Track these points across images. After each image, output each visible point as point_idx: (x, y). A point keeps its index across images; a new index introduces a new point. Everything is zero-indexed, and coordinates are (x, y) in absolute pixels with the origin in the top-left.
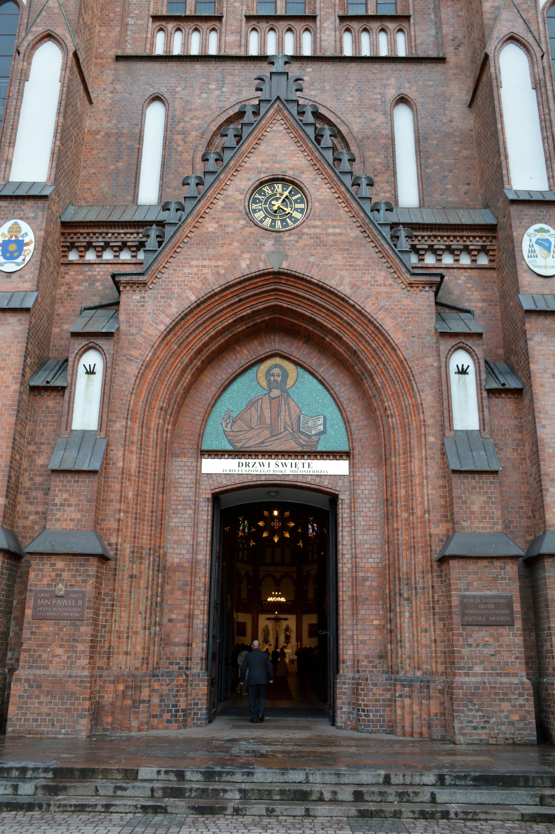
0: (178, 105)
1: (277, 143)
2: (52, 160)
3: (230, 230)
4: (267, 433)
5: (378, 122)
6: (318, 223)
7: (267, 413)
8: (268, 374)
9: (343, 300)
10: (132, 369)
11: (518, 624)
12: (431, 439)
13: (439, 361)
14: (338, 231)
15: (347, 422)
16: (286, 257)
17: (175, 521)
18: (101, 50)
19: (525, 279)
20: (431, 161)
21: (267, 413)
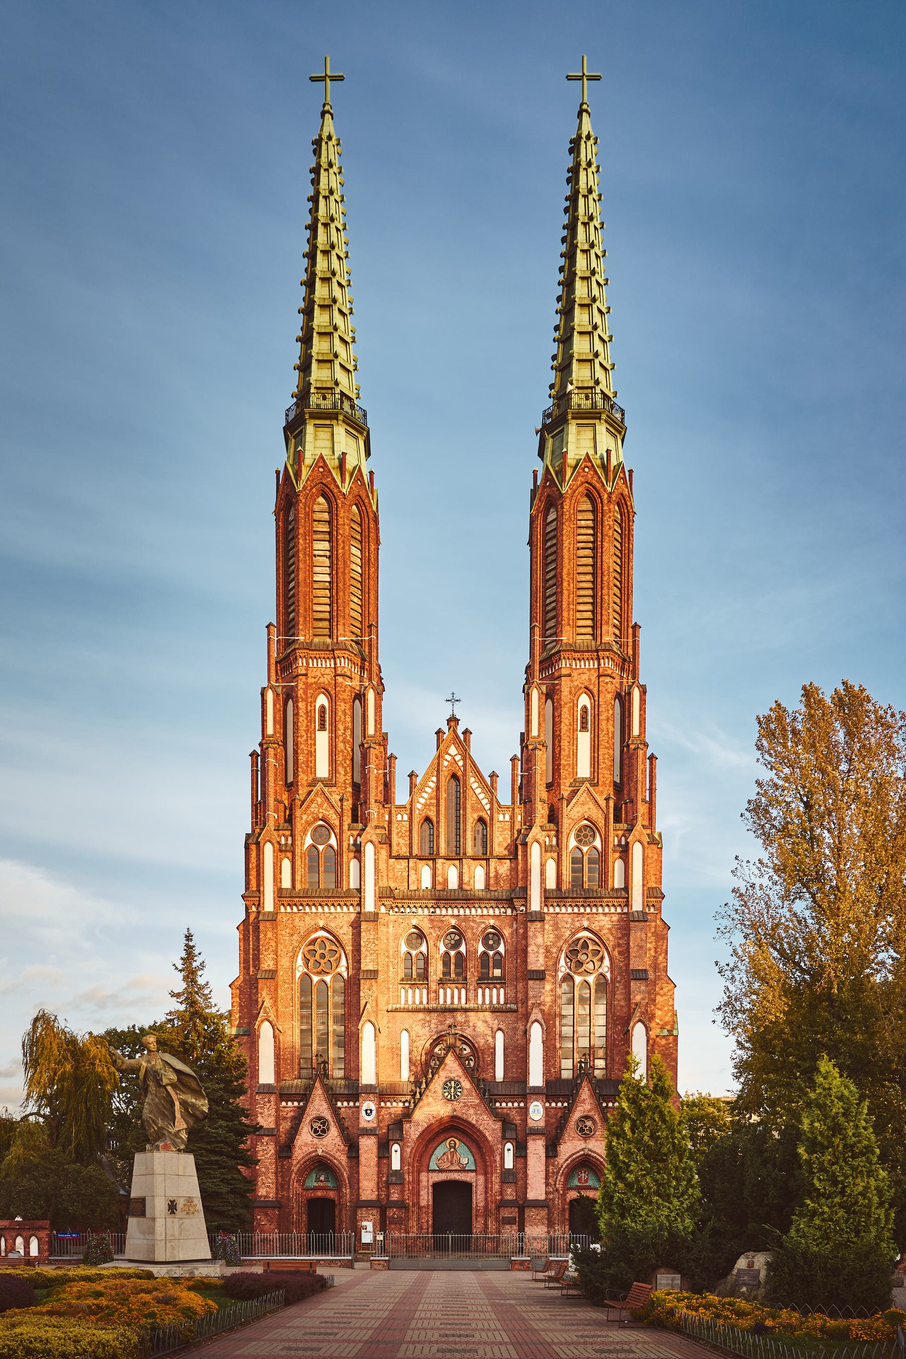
0: (413, 1034)
7: (450, 1157)
8: (450, 1143)
9: (473, 1126)
10: (409, 1150)
15: (475, 1160)
17: (422, 1193)
19: (529, 1121)
21: (450, 1157)
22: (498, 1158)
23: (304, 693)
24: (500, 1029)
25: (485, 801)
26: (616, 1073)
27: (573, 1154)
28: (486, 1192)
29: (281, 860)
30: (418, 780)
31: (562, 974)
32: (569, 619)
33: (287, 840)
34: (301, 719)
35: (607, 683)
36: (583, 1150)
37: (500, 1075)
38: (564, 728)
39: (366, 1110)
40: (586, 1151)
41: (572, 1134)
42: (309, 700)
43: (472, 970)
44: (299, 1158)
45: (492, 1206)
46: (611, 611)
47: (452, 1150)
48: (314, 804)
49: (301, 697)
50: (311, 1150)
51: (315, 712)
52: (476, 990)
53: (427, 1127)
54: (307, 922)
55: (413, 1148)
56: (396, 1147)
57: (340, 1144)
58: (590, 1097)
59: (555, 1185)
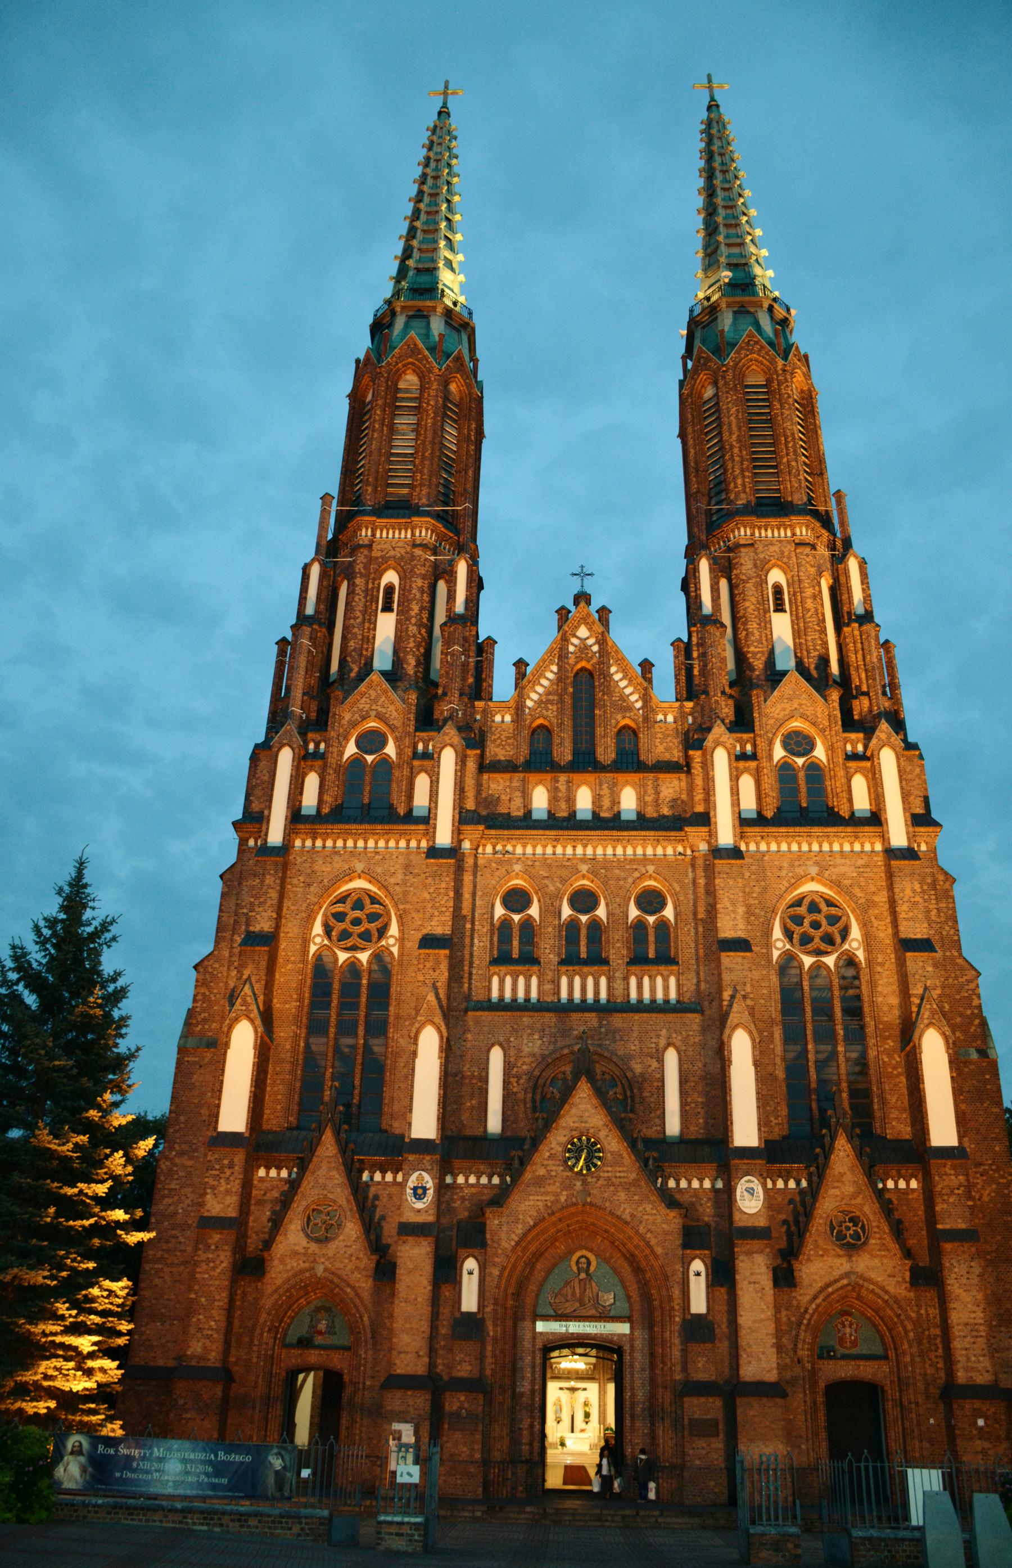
0: (512, 1052)
1: (582, 1107)
2: (438, 1124)
3: (553, 1173)
4: (577, 1304)
5: (652, 1068)
6: (610, 1169)
7: (577, 1290)
8: (578, 1262)
10: (496, 1272)
11: (721, 1436)
12: (677, 1319)
13: (683, 1267)
14: (622, 1175)
16: (590, 1195)
18: (455, 1004)
19: (737, 1217)
20: (689, 1100)
21: (577, 1290)
22: (676, 1292)
23: (364, 568)
24: (669, 1045)
25: (633, 698)
26: (893, 1127)
27: (828, 1285)
28: (652, 1366)
29: (304, 775)
30: (529, 669)
31: (779, 952)
32: (744, 485)
33: (317, 746)
34: (357, 598)
35: (807, 555)
36: (847, 1275)
37: (673, 1126)
38: (749, 605)
39: (415, 1189)
40: (853, 1277)
41: (821, 1242)
42: (372, 576)
43: (618, 945)
44: (279, 1282)
45: (666, 1397)
46: (801, 477)
47: (583, 1276)
48: (364, 699)
49: (360, 573)
50: (303, 1265)
51: (378, 591)
52: (626, 979)
53: (534, 1226)
54: (336, 866)
55: (504, 1268)
56: (471, 1264)
57: (361, 1255)
58: (852, 1169)
59: (795, 1350)
